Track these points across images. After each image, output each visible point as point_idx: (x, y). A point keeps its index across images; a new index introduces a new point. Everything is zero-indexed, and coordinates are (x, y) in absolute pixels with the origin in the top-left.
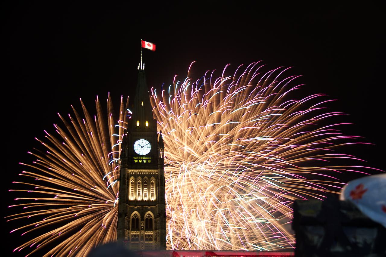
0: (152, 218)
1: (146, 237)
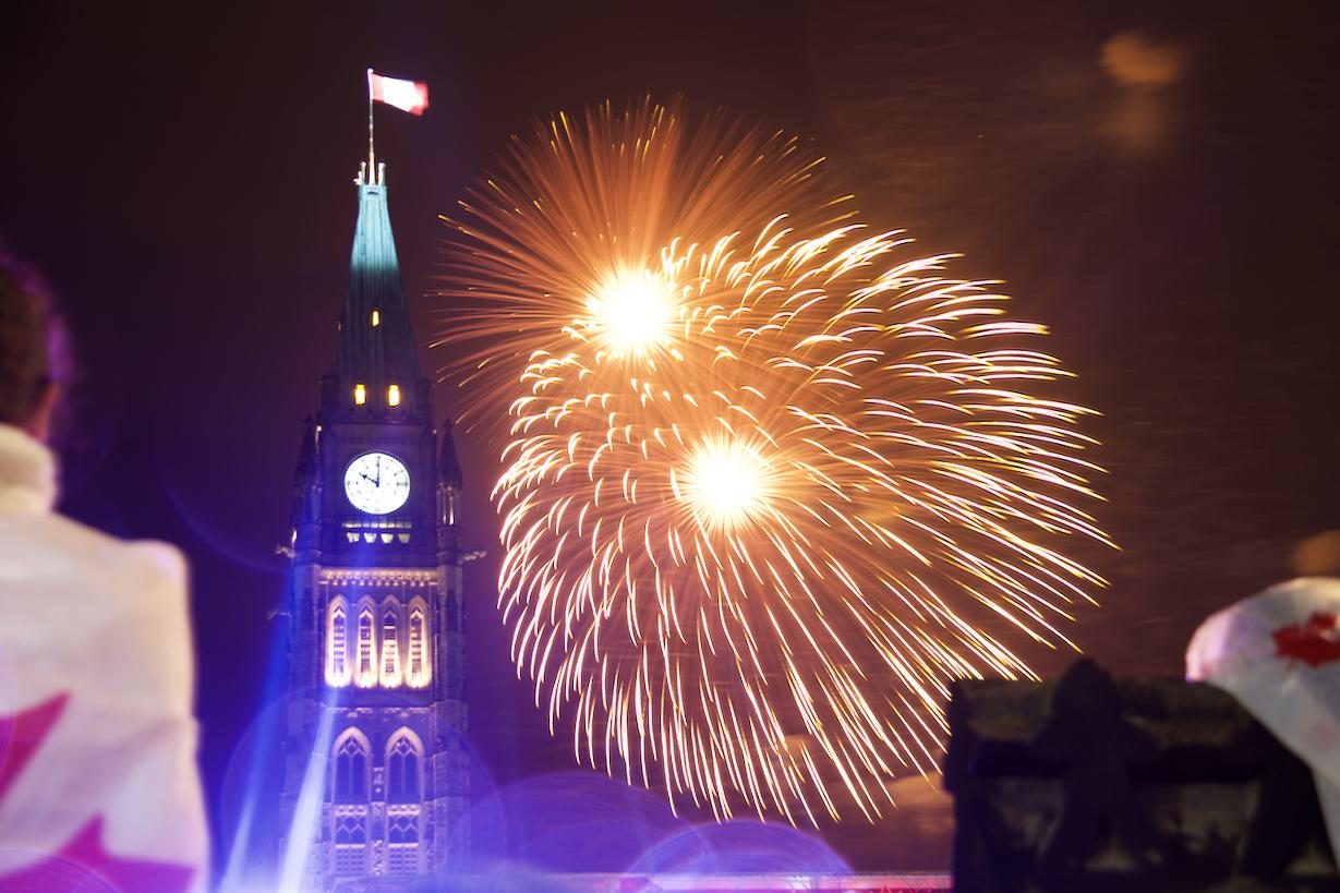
0: (365, 755)
1: (340, 828)
